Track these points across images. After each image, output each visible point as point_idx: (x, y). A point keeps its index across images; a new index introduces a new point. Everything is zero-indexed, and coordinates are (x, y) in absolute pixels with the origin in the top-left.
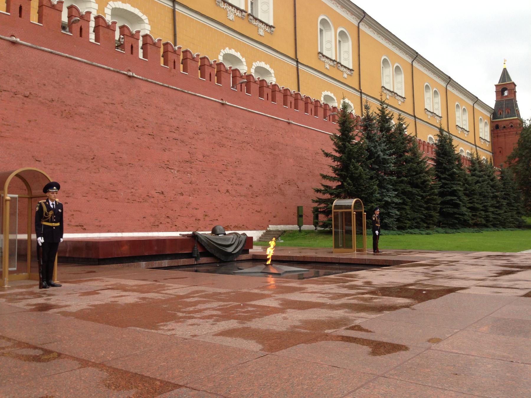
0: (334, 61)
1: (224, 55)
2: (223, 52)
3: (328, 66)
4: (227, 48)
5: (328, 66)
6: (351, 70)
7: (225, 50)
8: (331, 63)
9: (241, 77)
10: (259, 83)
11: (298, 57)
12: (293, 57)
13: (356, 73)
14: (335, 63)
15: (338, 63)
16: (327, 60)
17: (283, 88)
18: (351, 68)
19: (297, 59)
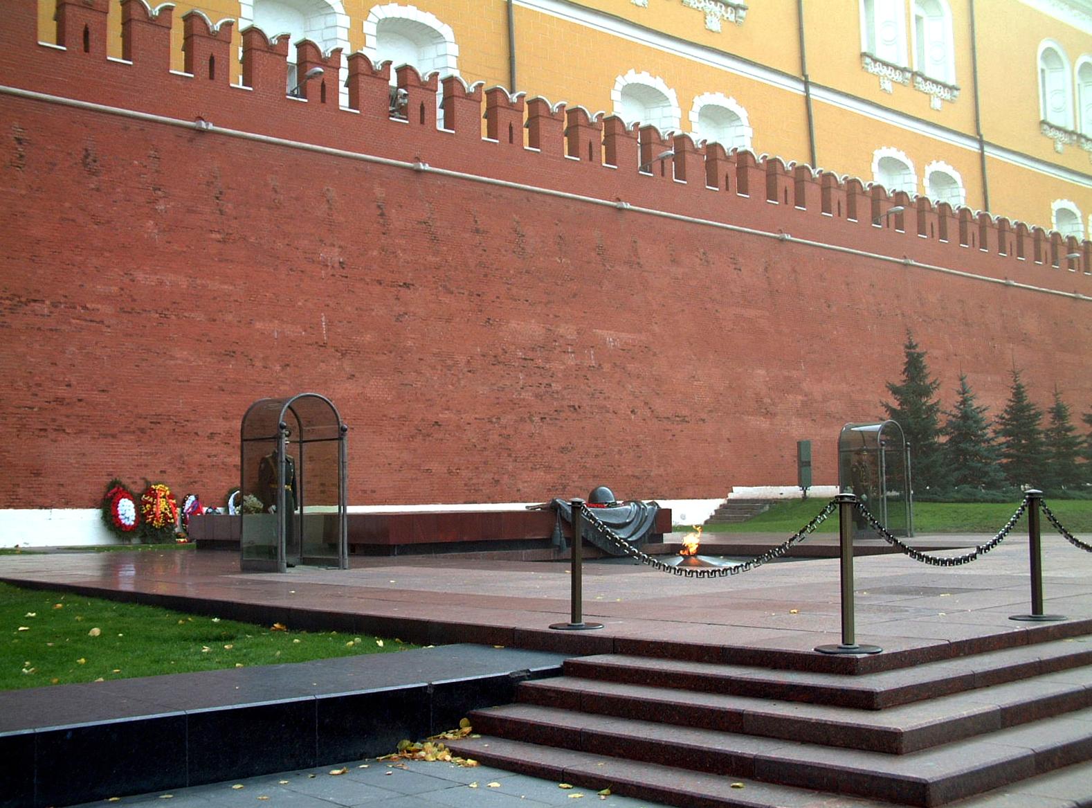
0: (904, 70)
1: (625, 87)
2: (621, 82)
3: (888, 86)
4: (631, 72)
5: (888, 86)
6: (952, 88)
7: (626, 77)
8: (898, 76)
9: (662, 143)
10: (735, 159)
11: (807, 72)
12: (796, 73)
13: (964, 96)
14: (908, 75)
15: (915, 74)
16: (885, 71)
17: (793, 164)
18: (951, 82)
19: (806, 77)
